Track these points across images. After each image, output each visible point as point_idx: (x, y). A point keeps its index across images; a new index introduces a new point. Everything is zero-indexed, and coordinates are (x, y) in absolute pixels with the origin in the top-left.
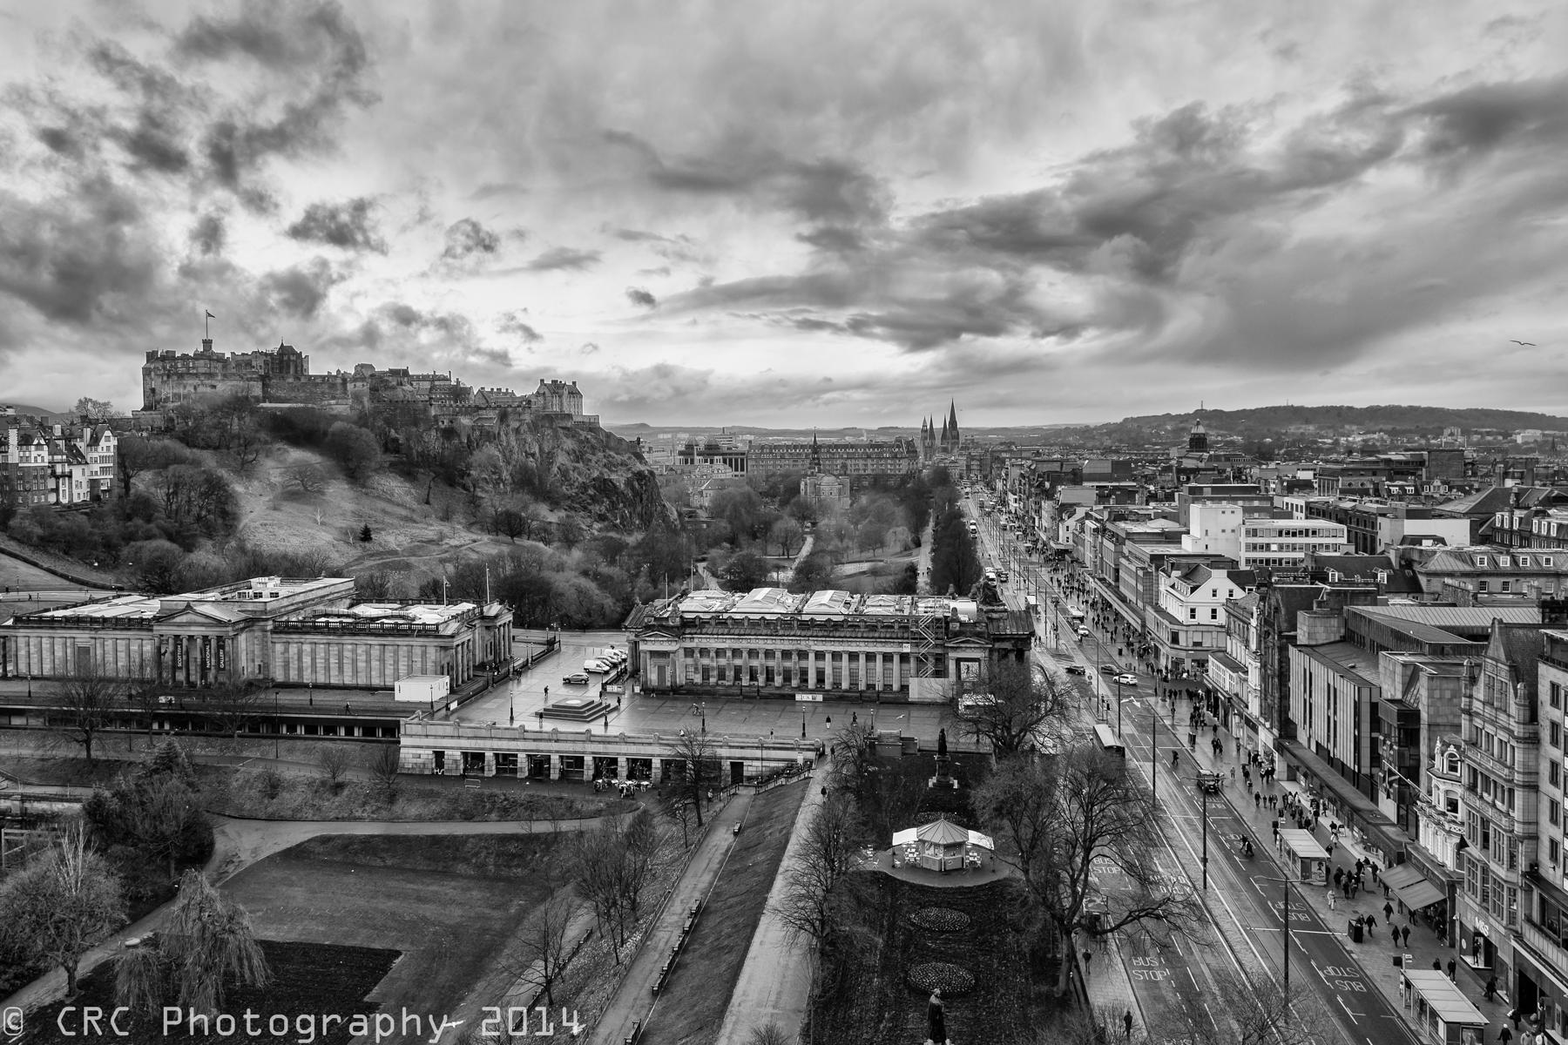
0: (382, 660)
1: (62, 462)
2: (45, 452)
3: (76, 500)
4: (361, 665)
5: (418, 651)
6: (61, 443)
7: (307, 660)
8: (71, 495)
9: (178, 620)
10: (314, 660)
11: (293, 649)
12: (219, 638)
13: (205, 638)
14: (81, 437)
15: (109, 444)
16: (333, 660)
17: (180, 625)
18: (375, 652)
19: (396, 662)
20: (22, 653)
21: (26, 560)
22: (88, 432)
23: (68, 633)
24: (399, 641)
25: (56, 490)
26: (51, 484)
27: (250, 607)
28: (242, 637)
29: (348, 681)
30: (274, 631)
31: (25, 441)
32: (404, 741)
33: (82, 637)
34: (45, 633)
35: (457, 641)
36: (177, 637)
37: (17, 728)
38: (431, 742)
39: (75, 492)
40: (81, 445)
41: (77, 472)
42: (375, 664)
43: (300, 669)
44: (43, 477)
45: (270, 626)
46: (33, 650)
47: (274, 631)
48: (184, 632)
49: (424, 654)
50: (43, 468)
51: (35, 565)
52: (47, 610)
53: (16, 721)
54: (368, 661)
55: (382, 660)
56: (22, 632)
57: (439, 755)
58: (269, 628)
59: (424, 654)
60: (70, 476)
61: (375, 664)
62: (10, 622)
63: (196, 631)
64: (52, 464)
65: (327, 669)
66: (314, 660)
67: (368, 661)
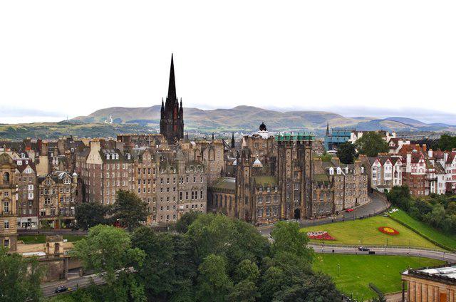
1: (432, 172)
3: (439, 193)
6: (432, 162)
20: (412, 290)
21: (414, 231)
22: (446, 155)
25: (429, 188)
31: (415, 161)
33: (443, 288)
34: (424, 281)
40: (442, 162)
41: (440, 177)
52: (425, 268)
56: (412, 279)
62: (406, 272)
64: (428, 172)
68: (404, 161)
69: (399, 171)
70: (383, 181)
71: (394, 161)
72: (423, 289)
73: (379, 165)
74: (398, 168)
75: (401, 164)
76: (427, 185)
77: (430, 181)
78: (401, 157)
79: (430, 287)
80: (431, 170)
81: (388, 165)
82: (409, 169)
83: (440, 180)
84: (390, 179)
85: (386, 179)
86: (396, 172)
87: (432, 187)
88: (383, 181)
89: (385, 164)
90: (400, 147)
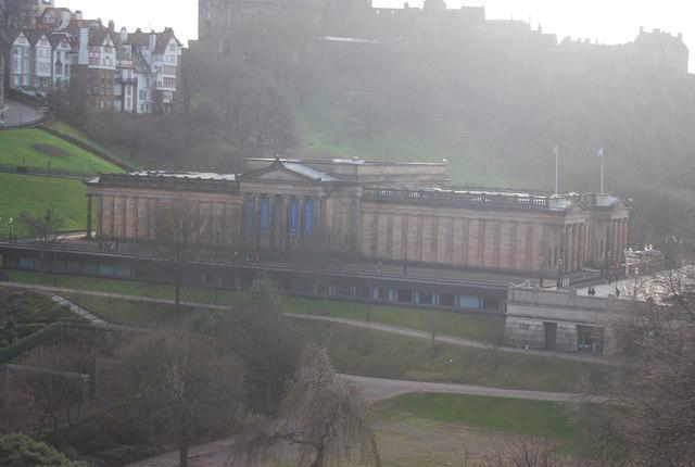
0: (481, 237)
2: (113, 55)
4: (458, 242)
5: (522, 229)
7: (397, 233)
8: (135, 104)
9: (265, 176)
10: (404, 233)
11: (383, 221)
12: (309, 199)
13: (293, 198)
14: (147, 44)
15: (171, 57)
16: (426, 235)
17: (267, 182)
18: (474, 228)
19: (497, 240)
23: (152, 194)
24: (502, 216)
25: (121, 98)
26: (117, 90)
27: (339, 171)
28: (329, 202)
29: (441, 260)
30: (364, 199)
32: (511, 309)
33: (166, 197)
35: (569, 221)
36: (264, 196)
37: (104, 277)
38: (543, 312)
39: (139, 102)
40: (146, 53)
42: (473, 242)
43: (390, 244)
44: (110, 81)
45: (359, 192)
46: (117, 209)
47: (364, 199)
48: (272, 190)
49: (530, 232)
50: (110, 72)
51: (106, 158)
53: (105, 270)
54: (466, 238)
55: (481, 237)
56: (107, 191)
57: (550, 327)
58: (359, 194)
59: (530, 232)
60: (135, 85)
61: (473, 242)
63: (283, 189)
64: (120, 68)
65: (419, 244)
66: (404, 233)
67: (466, 238)
68: (75, 43)
69: (64, 61)
70: (33, 76)
71: (54, 41)
72: (128, 207)
73: (27, 44)
74: (63, 55)
75: (69, 48)
76: (117, 90)
77: (123, 84)
78: (68, 35)
79: (142, 203)
80: (125, 63)
81: (43, 48)
82: (84, 58)
83: (141, 85)
84: (48, 74)
85: (39, 74)
86: (59, 63)
87: (126, 97)
88: (33, 76)
89: (38, 44)
90: (65, 24)
